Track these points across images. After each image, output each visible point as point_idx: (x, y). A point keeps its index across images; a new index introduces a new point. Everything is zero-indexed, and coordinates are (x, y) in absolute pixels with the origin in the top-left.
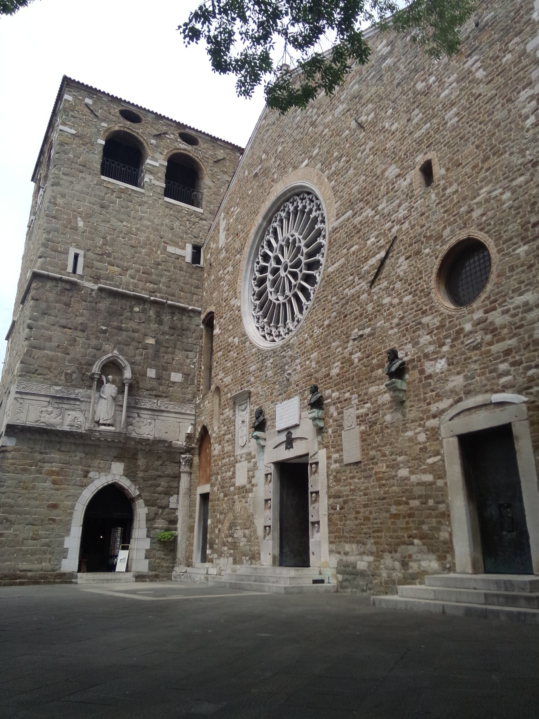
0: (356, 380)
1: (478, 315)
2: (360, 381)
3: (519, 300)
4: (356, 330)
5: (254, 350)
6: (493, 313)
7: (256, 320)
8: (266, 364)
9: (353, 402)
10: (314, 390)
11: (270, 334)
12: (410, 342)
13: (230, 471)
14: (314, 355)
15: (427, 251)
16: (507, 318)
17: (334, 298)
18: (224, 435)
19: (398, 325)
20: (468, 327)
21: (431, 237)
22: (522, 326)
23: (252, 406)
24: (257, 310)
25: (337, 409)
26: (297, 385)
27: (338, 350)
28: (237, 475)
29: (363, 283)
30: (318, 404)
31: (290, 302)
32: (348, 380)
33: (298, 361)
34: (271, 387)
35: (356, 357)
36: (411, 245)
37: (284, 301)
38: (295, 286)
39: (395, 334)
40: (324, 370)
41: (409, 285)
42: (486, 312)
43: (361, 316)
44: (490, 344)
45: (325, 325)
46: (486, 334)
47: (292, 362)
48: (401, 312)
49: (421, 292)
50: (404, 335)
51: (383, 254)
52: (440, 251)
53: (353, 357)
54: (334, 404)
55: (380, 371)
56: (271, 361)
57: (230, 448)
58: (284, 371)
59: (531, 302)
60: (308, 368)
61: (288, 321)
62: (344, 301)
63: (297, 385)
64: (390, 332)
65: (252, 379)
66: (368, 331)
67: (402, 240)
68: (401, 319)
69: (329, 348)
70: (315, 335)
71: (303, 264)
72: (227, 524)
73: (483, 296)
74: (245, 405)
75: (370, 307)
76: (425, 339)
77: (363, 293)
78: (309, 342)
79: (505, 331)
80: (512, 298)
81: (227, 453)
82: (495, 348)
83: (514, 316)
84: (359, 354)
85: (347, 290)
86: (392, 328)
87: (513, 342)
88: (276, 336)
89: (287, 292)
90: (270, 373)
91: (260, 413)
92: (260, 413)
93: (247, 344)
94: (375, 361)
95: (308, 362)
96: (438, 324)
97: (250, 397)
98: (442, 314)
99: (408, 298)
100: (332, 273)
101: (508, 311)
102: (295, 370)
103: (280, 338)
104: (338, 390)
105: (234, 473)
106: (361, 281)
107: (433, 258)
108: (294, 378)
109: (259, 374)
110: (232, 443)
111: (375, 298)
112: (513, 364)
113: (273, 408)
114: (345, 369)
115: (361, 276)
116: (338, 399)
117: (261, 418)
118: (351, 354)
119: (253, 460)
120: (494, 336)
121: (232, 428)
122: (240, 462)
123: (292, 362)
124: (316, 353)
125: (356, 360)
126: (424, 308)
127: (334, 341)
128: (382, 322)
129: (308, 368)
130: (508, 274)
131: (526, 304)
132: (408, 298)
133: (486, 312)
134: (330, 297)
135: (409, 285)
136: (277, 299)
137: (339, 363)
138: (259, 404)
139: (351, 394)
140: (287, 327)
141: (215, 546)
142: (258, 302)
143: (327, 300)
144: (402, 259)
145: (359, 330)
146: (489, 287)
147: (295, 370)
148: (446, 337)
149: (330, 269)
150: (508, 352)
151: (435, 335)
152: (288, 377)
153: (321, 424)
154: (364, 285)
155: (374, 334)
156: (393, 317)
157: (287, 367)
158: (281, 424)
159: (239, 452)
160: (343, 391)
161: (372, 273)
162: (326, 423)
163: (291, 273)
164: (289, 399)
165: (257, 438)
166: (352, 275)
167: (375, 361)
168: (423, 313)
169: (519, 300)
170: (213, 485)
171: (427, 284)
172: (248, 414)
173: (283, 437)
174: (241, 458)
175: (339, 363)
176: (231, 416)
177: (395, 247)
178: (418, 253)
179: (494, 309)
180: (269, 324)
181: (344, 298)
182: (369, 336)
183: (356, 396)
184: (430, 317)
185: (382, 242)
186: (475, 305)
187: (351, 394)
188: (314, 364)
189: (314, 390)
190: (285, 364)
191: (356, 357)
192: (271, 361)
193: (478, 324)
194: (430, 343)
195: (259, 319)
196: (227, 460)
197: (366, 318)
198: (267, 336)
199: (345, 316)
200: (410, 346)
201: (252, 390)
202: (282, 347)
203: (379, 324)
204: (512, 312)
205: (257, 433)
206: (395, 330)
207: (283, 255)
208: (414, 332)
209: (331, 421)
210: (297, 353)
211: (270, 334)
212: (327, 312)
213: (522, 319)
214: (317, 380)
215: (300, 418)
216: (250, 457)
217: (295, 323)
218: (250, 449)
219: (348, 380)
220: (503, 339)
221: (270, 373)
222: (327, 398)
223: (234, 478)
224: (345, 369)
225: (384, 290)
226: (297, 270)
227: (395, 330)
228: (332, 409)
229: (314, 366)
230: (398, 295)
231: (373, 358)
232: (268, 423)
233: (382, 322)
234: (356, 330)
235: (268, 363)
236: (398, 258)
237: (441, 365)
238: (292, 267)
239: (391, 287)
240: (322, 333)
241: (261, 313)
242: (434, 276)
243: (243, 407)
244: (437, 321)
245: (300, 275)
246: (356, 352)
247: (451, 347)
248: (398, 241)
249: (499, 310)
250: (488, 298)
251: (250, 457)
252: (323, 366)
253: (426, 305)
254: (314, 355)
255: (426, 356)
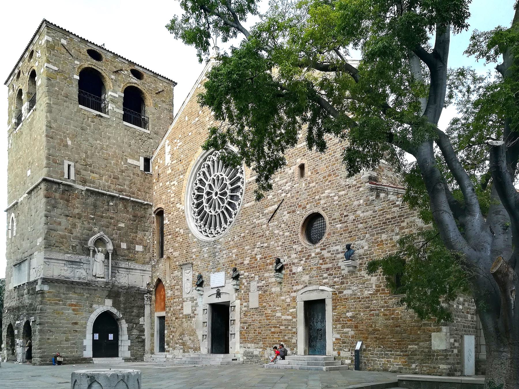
0: (258, 268)
1: (318, 250)
2: (260, 269)
3: (335, 248)
4: (259, 243)
5: (195, 239)
6: (324, 251)
7: (195, 221)
8: (203, 250)
9: (256, 279)
10: (235, 270)
11: (205, 231)
12: (286, 256)
13: (179, 306)
14: (235, 251)
15: (298, 212)
16: (329, 255)
17: (248, 222)
18: (174, 286)
19: (281, 246)
20: (313, 255)
21: (300, 206)
22: (335, 259)
23: (194, 272)
24: (196, 214)
25: (247, 281)
26: (224, 265)
27: (248, 251)
28: (184, 308)
29: (264, 219)
30: (236, 278)
31: (219, 214)
32: (254, 267)
33: (224, 252)
34: (207, 263)
35: (259, 257)
36: (291, 206)
37: (215, 214)
38: (223, 207)
39: (279, 250)
40: (240, 260)
41: (289, 227)
42: (321, 250)
43: (263, 236)
44: (321, 264)
45: (242, 236)
46: (320, 259)
47: (220, 251)
48: (283, 240)
49: (294, 232)
50: (284, 252)
51: (276, 206)
52: (304, 215)
53: (257, 256)
54: (245, 278)
55: (271, 266)
56: (207, 248)
57: (179, 293)
58: (215, 256)
59: (340, 250)
60: (230, 257)
61: (217, 226)
62: (253, 226)
63: (224, 265)
64: (277, 248)
65: (194, 257)
66: (266, 245)
67: (286, 202)
68: (283, 243)
69: (244, 249)
70: (235, 240)
71: (228, 195)
72: (178, 334)
73: (321, 242)
74: (189, 270)
75: (267, 232)
76: (294, 256)
77: (264, 224)
78: (232, 243)
79: (328, 260)
80: (332, 246)
81: (177, 296)
82: (323, 267)
83: (332, 254)
84: (260, 256)
85: (255, 220)
86: (278, 246)
87: (330, 265)
88: (209, 234)
89: (217, 209)
90: (206, 255)
91: (200, 277)
92: (200, 277)
93: (190, 235)
94: (268, 261)
95: (230, 254)
96: (300, 250)
97: (192, 266)
98: (303, 245)
99: (287, 234)
100: (247, 207)
101: (330, 251)
102: (223, 256)
103: (212, 235)
104: (248, 272)
105: (182, 307)
106: (263, 217)
107: (301, 217)
108: (222, 261)
109: (198, 254)
110: (180, 291)
111: (271, 229)
112: (329, 275)
113: (208, 275)
114: (252, 262)
115: (264, 214)
116: (247, 276)
117: (201, 280)
118: (256, 255)
119: (195, 302)
120: (323, 261)
121: (180, 283)
122: (186, 301)
123: (220, 251)
124: (236, 250)
125: (259, 259)
126: (295, 241)
127: (247, 245)
128: (274, 242)
129: (230, 257)
130: (332, 235)
131: (337, 250)
132: (287, 234)
133: (321, 250)
134: (245, 221)
135: (289, 227)
136: (210, 212)
137: (249, 258)
138: (199, 271)
139: (255, 275)
140: (217, 229)
141: (170, 344)
142: (197, 210)
143: (243, 222)
144: (285, 213)
145: (261, 243)
146: (324, 239)
147: (223, 256)
148: (303, 257)
149: (246, 205)
150: (328, 269)
151: (299, 254)
152: (218, 260)
153: (238, 287)
154: (264, 220)
155: (269, 247)
156: (279, 241)
157: (217, 254)
158: (213, 285)
159: (185, 296)
160: (250, 273)
161: (270, 215)
162: (240, 287)
163: (220, 198)
164: (218, 271)
165: (199, 290)
166: (258, 212)
167: (268, 261)
168: (294, 243)
169: (335, 248)
170: (166, 313)
171: (297, 229)
172: (191, 276)
173: (215, 291)
174: (187, 299)
175: (249, 258)
176: (179, 276)
177: (283, 204)
178: (294, 211)
179: (325, 249)
180: (205, 225)
181: (253, 224)
182: (266, 247)
183: (258, 276)
184: (297, 246)
185: (275, 200)
186: (317, 245)
187: (255, 275)
188: (234, 256)
189: (235, 270)
190: (216, 252)
191: (259, 257)
192: (207, 248)
193: (317, 254)
194: (296, 258)
195: (197, 220)
196: (177, 300)
197: (265, 238)
198: (203, 233)
199: (254, 234)
200: (286, 257)
201: (194, 262)
202: (214, 242)
203: (272, 243)
204: (332, 252)
205: (198, 288)
206: (280, 248)
207: (214, 184)
208: (289, 251)
209: (243, 287)
210: (224, 247)
211: (205, 231)
212: (243, 229)
213: (335, 257)
214: (236, 265)
215: (225, 283)
216: (193, 299)
217: (222, 229)
218: (193, 296)
219: (254, 267)
220: (327, 263)
221: (206, 255)
222: (242, 275)
223: (182, 310)
224: (252, 262)
225: (275, 226)
226: (224, 198)
227: (280, 248)
228: (244, 281)
229: (235, 257)
230: (282, 231)
231: (268, 259)
232: (205, 283)
233: (274, 242)
234: (259, 243)
235: (205, 249)
236: (284, 211)
237: (300, 269)
238: (221, 194)
239: (279, 225)
240: (240, 240)
241: (199, 217)
242: (300, 226)
243: (188, 271)
244: (299, 249)
245: (226, 202)
246: (259, 254)
247: (305, 262)
248: (284, 202)
249: (327, 250)
250: (323, 243)
251: (193, 299)
252: (240, 258)
253: (296, 239)
254: (235, 251)
255: (294, 264)
